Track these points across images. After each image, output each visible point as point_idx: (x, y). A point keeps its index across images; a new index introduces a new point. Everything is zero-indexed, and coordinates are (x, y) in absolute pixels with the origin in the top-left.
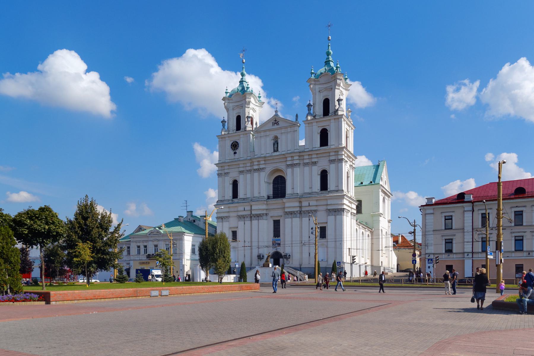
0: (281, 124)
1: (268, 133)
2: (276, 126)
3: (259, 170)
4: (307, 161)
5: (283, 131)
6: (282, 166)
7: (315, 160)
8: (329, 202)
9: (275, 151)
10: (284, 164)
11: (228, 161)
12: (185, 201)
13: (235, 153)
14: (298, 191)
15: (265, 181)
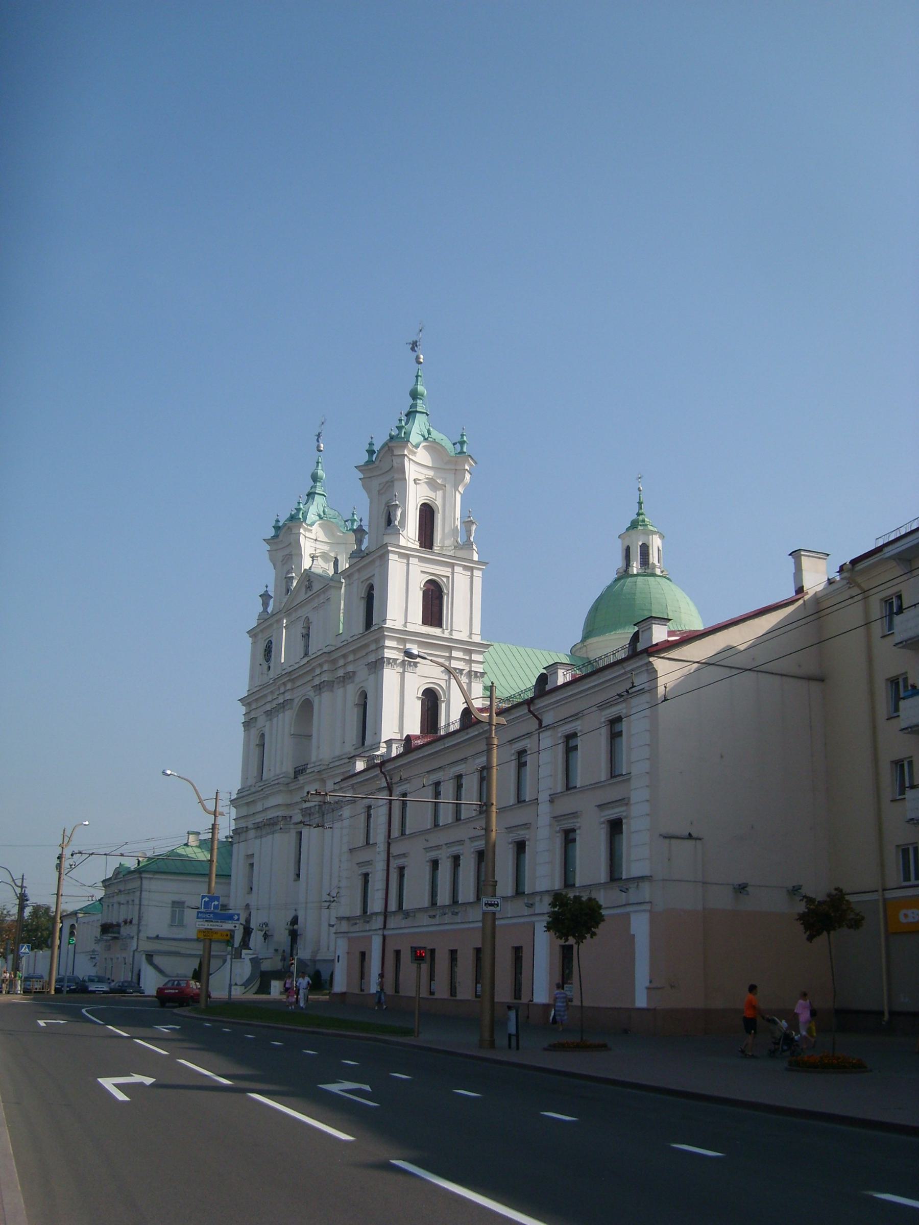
0: (316, 587)
2: (310, 593)
3: (282, 706)
5: (315, 603)
7: (350, 668)
10: (309, 687)
11: (258, 689)
12: (227, 793)
15: (292, 733)
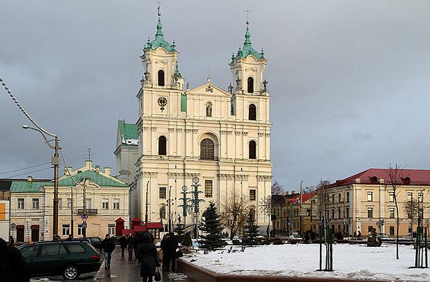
1: (201, 97)
2: (209, 93)
4: (239, 131)
6: (217, 133)
8: (260, 169)
9: (207, 115)
13: (162, 109)
14: (231, 155)
